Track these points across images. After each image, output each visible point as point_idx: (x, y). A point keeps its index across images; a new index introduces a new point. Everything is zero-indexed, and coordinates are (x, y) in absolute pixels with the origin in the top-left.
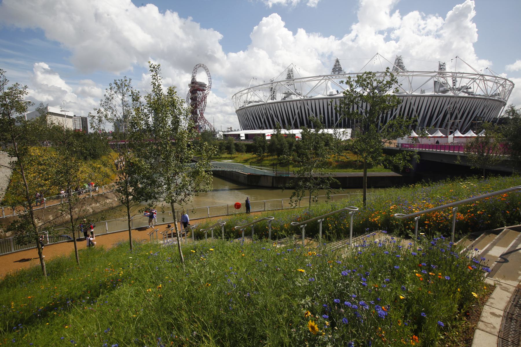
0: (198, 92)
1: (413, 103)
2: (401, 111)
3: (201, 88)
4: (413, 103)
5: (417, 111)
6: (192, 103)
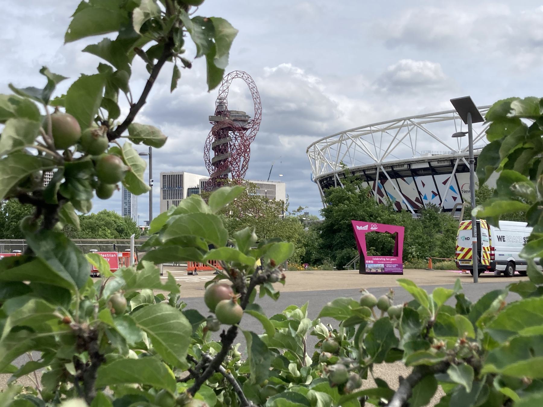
3: (239, 125)
6: (216, 160)
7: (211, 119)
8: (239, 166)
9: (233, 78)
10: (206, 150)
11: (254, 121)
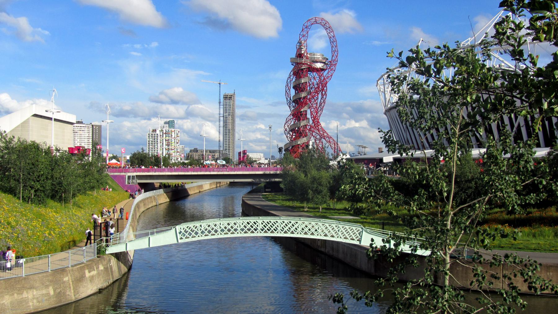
8: (317, 104)
9: (312, 24)
10: (287, 89)
11: (331, 62)
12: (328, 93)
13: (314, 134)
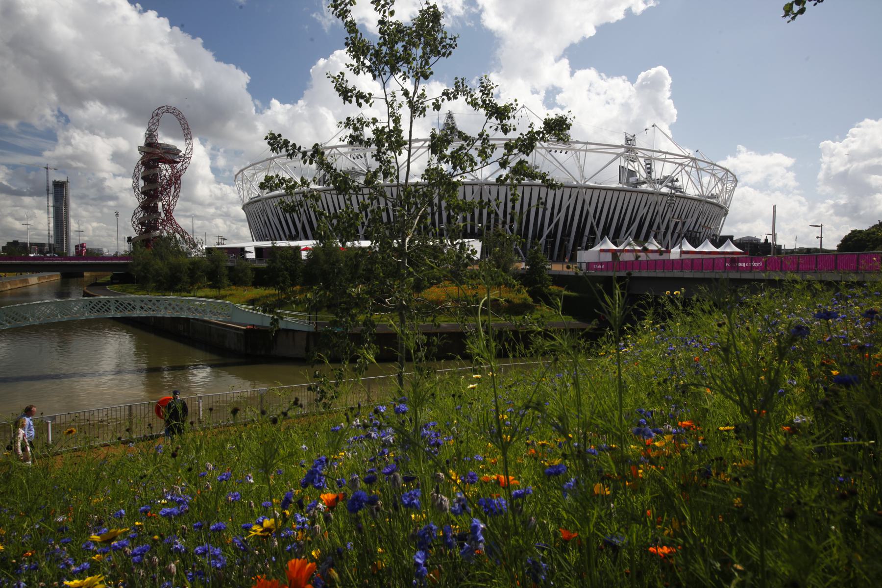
0: (161, 165)
1: (587, 201)
2: (567, 216)
3: (170, 157)
4: (587, 201)
5: (594, 217)
6: (147, 188)
7: (140, 149)
12: (182, 186)
13: (166, 228)
